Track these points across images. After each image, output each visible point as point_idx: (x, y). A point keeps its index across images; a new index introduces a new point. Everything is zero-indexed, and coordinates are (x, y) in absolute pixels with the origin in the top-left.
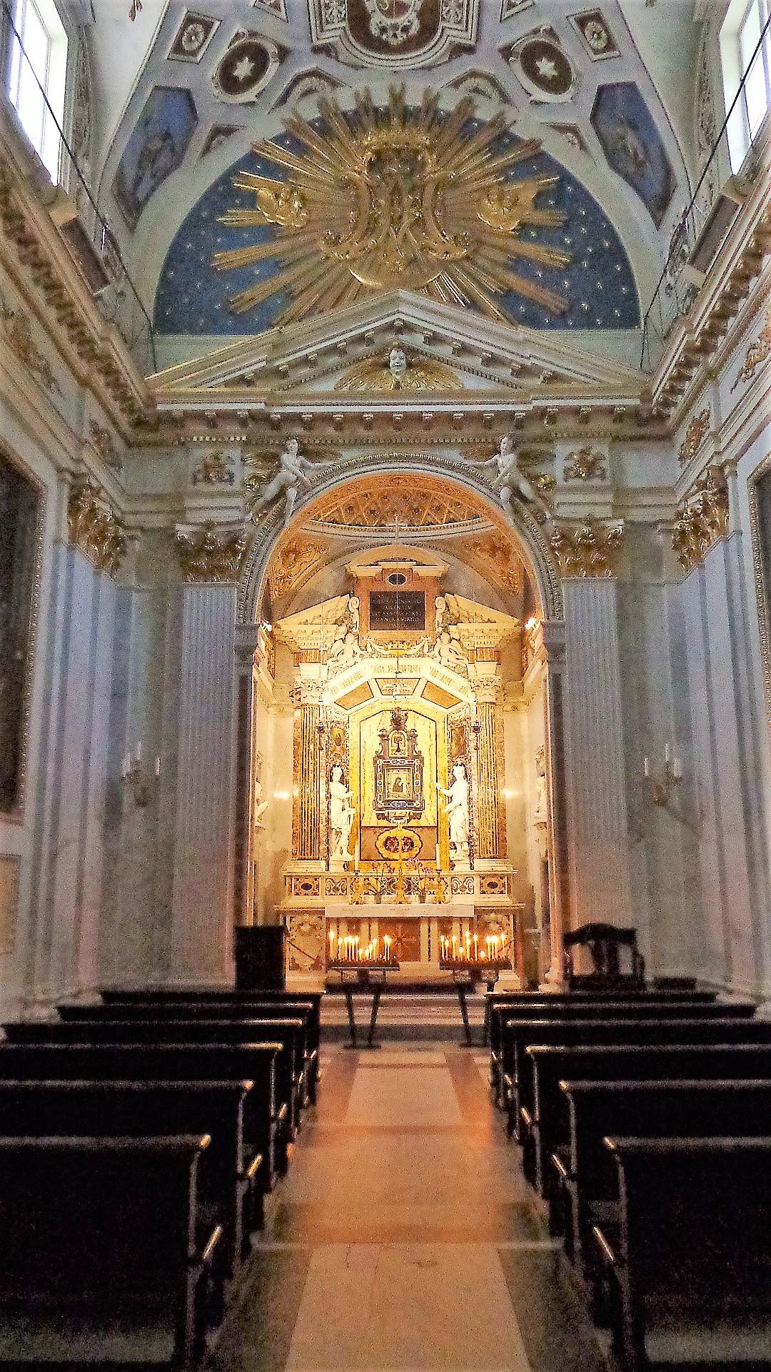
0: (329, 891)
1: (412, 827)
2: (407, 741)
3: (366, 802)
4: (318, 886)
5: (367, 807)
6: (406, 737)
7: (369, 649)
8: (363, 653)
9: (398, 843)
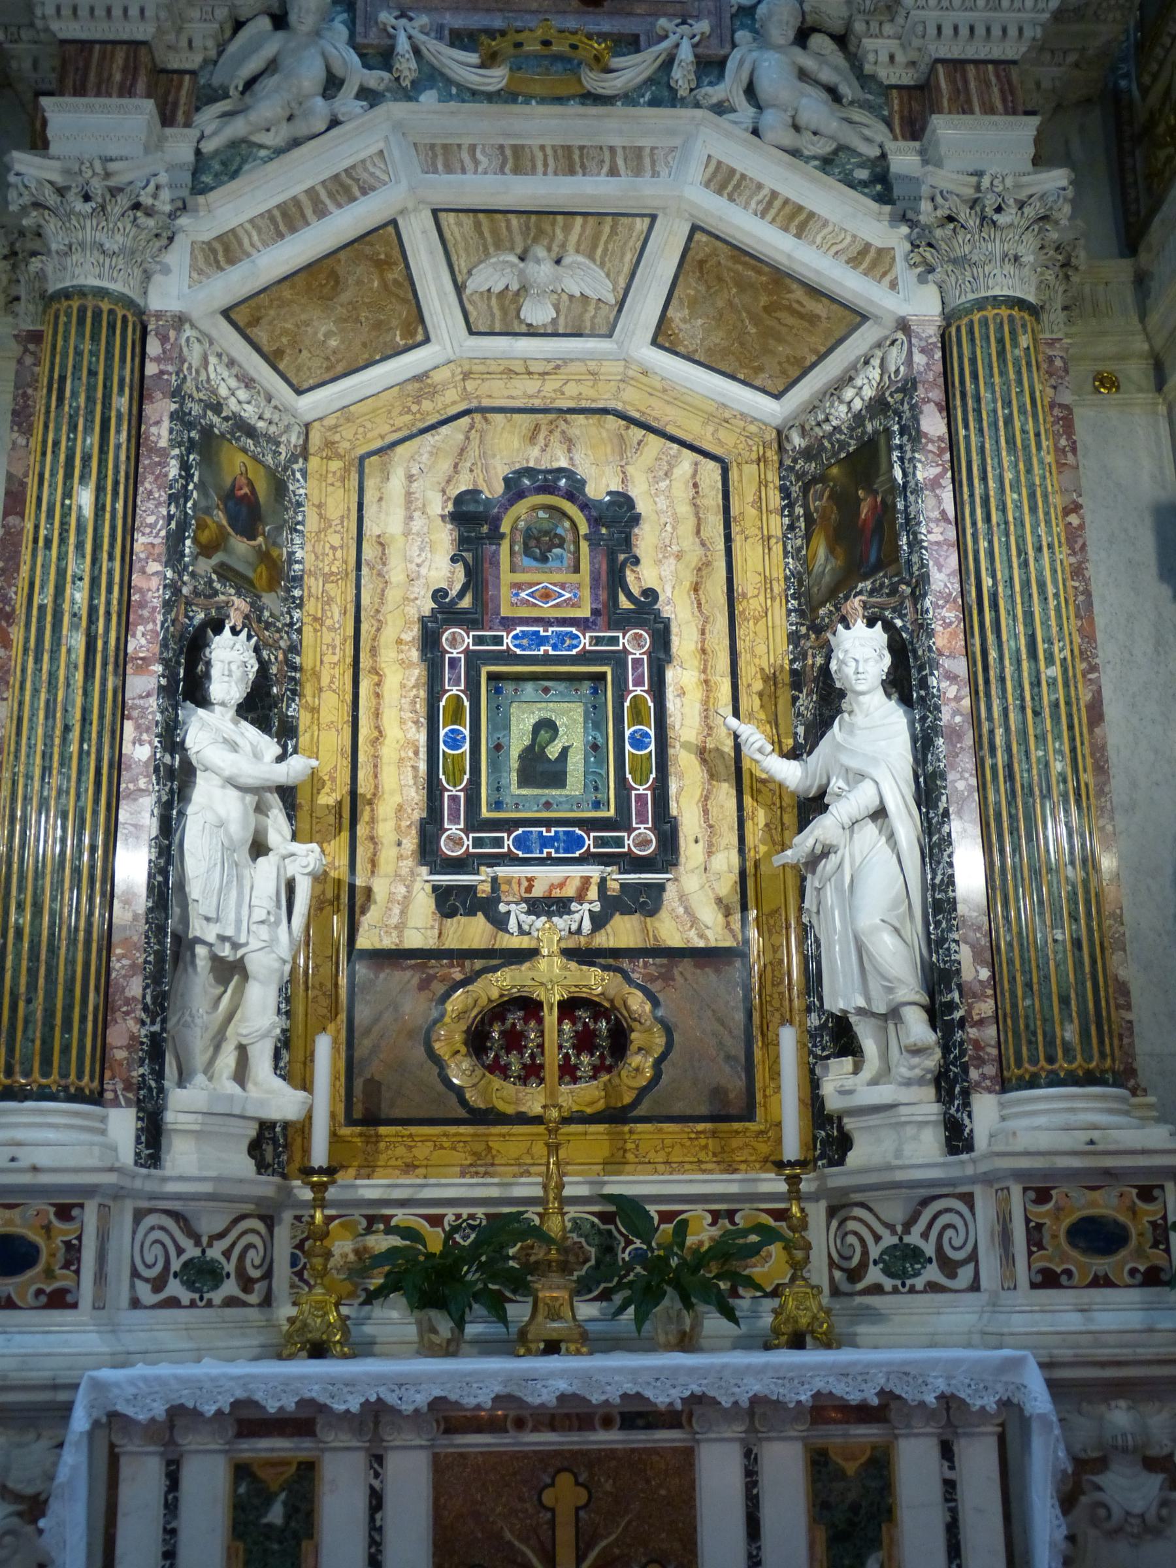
0: (158, 1284)
1: (616, 953)
2: (584, 546)
3: (386, 830)
4: (73, 1251)
5: (388, 854)
6: (584, 529)
7: (407, 66)
8: (375, 79)
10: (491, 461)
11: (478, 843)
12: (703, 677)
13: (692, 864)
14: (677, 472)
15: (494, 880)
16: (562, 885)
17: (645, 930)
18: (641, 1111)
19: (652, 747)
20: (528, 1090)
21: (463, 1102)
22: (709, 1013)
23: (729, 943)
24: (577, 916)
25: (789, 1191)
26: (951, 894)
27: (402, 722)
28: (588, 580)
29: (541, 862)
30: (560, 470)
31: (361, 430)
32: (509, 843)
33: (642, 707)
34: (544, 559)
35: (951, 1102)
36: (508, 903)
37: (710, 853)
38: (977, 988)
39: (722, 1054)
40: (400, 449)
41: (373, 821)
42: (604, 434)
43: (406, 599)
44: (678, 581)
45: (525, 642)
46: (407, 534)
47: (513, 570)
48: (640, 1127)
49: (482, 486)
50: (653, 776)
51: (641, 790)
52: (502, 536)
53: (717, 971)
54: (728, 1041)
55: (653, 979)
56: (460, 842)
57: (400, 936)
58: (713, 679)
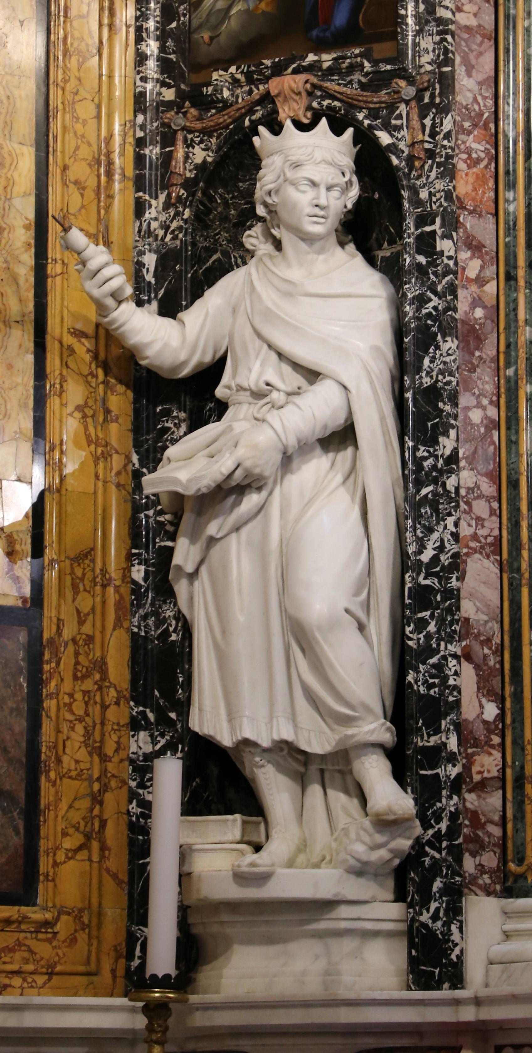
25: (150, 1028)
26: (454, 583)
35: (425, 904)
38: (480, 731)
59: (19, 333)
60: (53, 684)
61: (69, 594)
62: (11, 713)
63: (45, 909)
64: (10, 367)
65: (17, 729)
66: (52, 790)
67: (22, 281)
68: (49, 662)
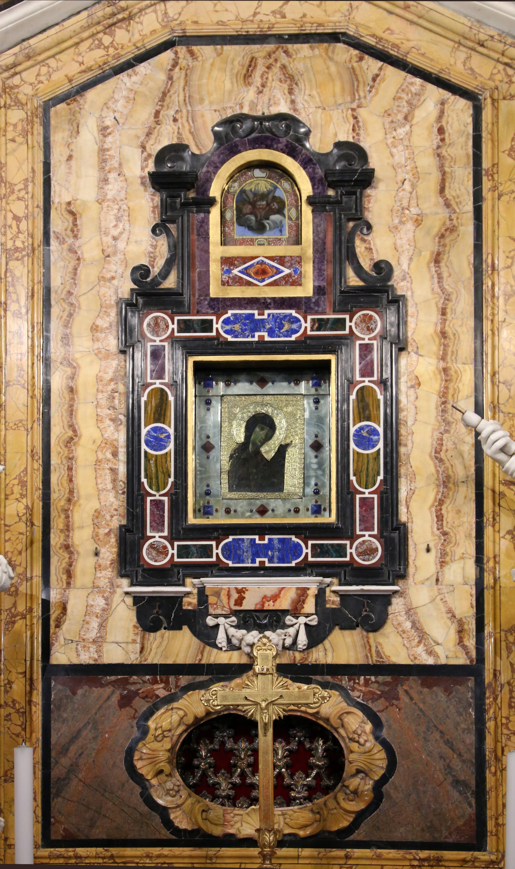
2: (307, 211)
9: (255, 752)
10: (198, 108)
11: (183, 552)
12: (442, 364)
13: (421, 576)
14: (419, 114)
15: (202, 592)
16: (275, 597)
17: (367, 646)
18: (356, 836)
19: (381, 445)
20: (237, 811)
21: (168, 823)
22: (437, 735)
23: (462, 660)
24: (292, 631)
27: (99, 419)
28: (310, 252)
29: (253, 572)
30: (281, 117)
31: (44, 70)
32: (217, 551)
33: (369, 400)
34: (260, 229)
36: (216, 616)
37: (443, 563)
39: (450, 779)
40: (91, 94)
41: (68, 528)
42: (333, 69)
43: (102, 279)
44: (416, 251)
45: (237, 327)
46: (100, 202)
47: (224, 243)
48: (358, 852)
49: (188, 140)
50: (381, 477)
51: (367, 493)
52: (212, 202)
53: (448, 691)
54: (457, 764)
55: (374, 698)
56: (164, 551)
57: (99, 651)
58: (454, 367)
59: (465, 489)
60: (492, 711)
61: (504, 653)
62: (463, 732)
63: (491, 853)
64: (459, 512)
65: (468, 741)
66: (493, 779)
67: (466, 455)
68: (489, 698)
